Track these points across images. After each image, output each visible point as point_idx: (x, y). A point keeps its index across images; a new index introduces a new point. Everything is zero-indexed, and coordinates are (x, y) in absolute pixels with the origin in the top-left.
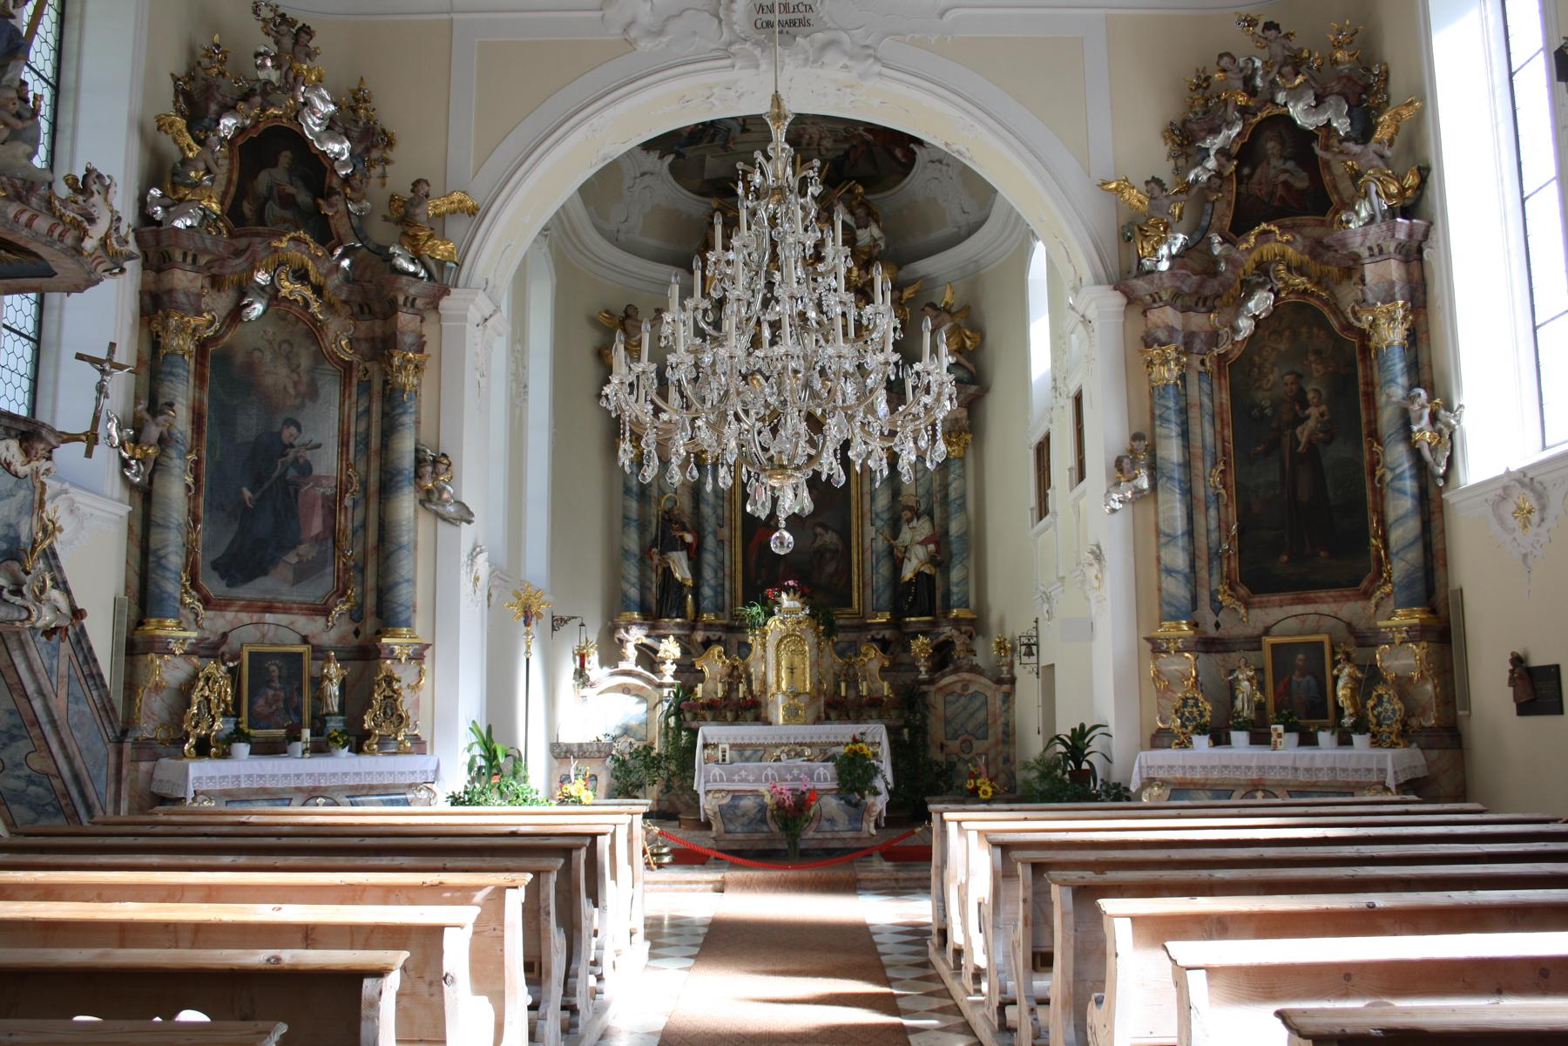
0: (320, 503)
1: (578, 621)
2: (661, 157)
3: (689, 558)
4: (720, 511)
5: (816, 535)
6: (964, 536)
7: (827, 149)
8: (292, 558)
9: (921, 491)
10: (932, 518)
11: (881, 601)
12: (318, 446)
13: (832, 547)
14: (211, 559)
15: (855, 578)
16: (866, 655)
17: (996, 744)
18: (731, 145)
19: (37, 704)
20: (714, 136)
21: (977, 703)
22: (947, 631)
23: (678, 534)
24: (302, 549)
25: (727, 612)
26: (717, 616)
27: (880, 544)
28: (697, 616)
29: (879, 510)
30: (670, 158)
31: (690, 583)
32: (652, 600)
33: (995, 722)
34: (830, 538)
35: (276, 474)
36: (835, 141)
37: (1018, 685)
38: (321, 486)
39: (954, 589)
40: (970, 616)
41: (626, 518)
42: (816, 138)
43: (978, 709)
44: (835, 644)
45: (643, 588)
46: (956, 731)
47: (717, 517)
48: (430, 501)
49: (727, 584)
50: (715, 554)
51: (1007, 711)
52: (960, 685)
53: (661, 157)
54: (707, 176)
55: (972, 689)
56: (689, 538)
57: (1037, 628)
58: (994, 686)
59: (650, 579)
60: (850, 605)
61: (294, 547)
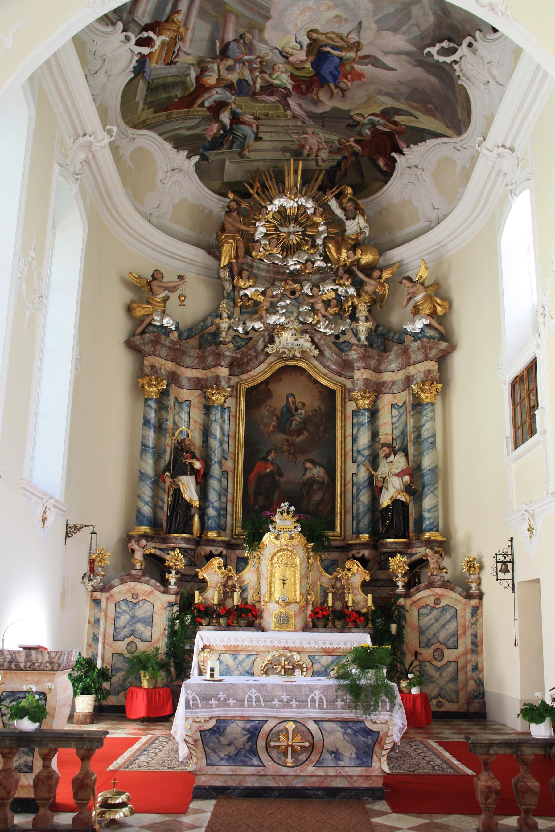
1: (90, 529)
2: (189, 157)
3: (197, 483)
4: (225, 446)
5: (306, 470)
6: (434, 470)
7: (323, 161)
9: (397, 433)
10: (406, 455)
11: (361, 525)
13: (318, 479)
15: (338, 506)
16: (349, 570)
17: (465, 654)
18: (246, 152)
20: (233, 142)
21: (448, 616)
22: (420, 551)
23: (188, 461)
25: (228, 532)
26: (219, 535)
27: (363, 474)
28: (202, 533)
29: (360, 448)
30: (196, 158)
31: (196, 503)
32: (163, 516)
33: (465, 633)
34: (317, 472)
36: (330, 152)
37: (485, 598)
39: (426, 515)
40: (440, 538)
41: (143, 445)
42: (315, 148)
43: (449, 621)
44: (322, 561)
45: (155, 507)
46: (429, 640)
47: (223, 451)
49: (229, 508)
50: (220, 481)
51: (475, 623)
52: (433, 599)
53: (189, 157)
54: (225, 180)
55: (443, 604)
56: (197, 465)
57: (512, 547)
58: (464, 601)
59: (162, 500)
60: (333, 529)
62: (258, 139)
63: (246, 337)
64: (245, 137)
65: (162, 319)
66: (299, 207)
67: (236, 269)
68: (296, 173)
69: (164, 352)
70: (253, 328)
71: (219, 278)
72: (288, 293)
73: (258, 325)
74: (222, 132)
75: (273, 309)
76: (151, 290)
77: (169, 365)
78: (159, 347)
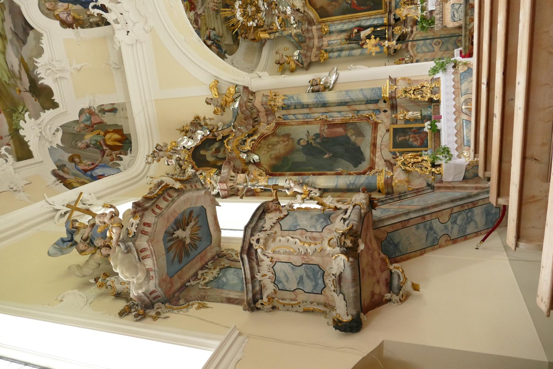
0: (330, 130)
8: (353, 138)
12: (308, 132)
14: (353, 167)
18: (220, 35)
19: (413, 215)
20: (217, 40)
24: (349, 135)
30: (226, 55)
35: (319, 147)
38: (324, 130)
42: (214, 4)
48: (329, 87)
54: (232, 43)
61: (349, 138)
62: (214, 29)
63: (298, 23)
64: (215, 35)
65: (295, 56)
66: (239, 8)
67: (270, 31)
68: (225, 11)
69: (309, 54)
70: (294, 20)
71: (274, 39)
72: (277, 7)
73: (292, 18)
74: (214, 45)
75: (285, 13)
76: (283, 63)
77: (314, 50)
78: (307, 55)
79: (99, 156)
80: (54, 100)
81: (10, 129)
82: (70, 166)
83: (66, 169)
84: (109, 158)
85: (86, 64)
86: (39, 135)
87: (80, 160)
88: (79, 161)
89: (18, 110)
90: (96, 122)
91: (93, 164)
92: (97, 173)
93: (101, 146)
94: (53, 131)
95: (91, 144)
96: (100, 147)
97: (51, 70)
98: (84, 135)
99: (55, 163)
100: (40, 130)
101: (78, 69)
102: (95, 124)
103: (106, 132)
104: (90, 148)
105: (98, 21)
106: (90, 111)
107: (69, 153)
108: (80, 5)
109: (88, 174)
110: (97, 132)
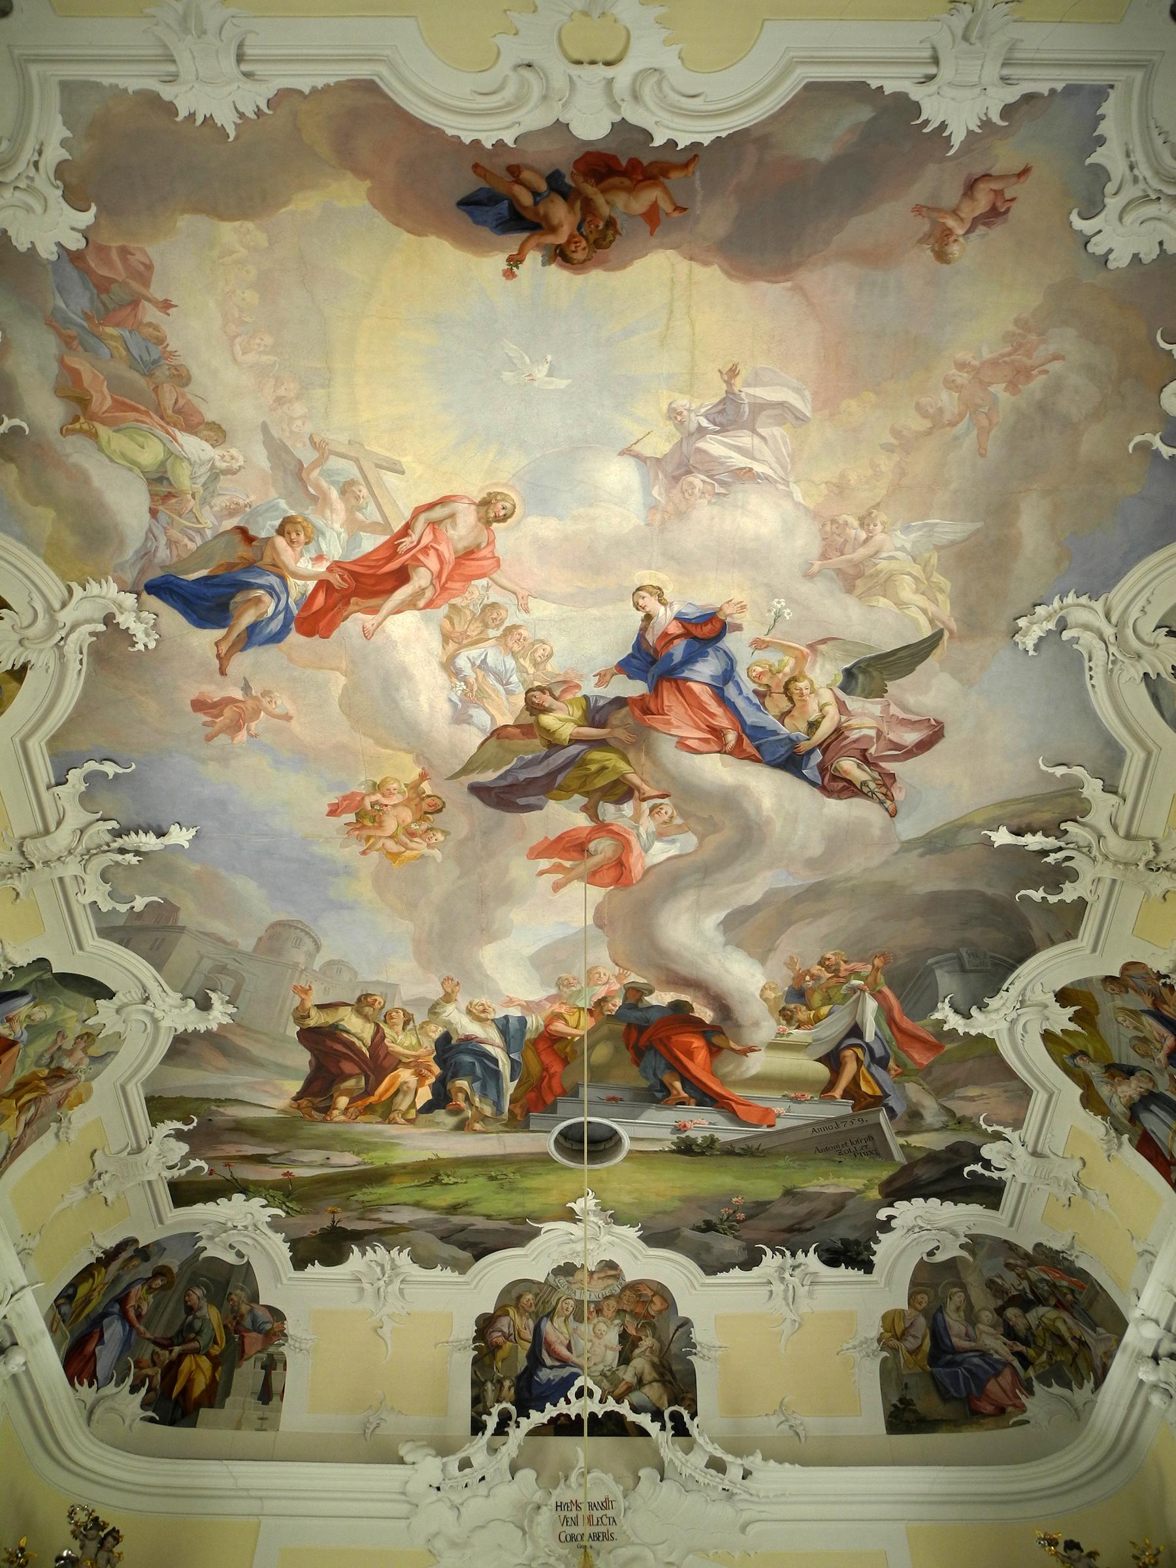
79: (159, 1332)
80: (313, 1265)
81: (247, 1181)
82: (146, 1270)
83: (135, 1262)
84: (147, 1357)
85: (389, 1347)
86: (230, 1224)
87: (156, 1289)
88: (153, 1286)
89: (290, 1202)
90: (247, 1341)
91: (139, 1316)
92: (110, 1325)
93: (184, 1342)
94: (239, 1247)
95: (195, 1318)
96: (181, 1340)
97: (381, 1276)
98: (220, 1307)
99: (157, 1243)
100: (239, 1227)
101: (379, 1330)
102: (242, 1338)
103: (215, 1362)
104: (183, 1315)
105: (485, 1402)
106: (275, 1334)
107: (180, 1269)
108: (527, 1368)
109: (113, 1307)
110: (221, 1338)
